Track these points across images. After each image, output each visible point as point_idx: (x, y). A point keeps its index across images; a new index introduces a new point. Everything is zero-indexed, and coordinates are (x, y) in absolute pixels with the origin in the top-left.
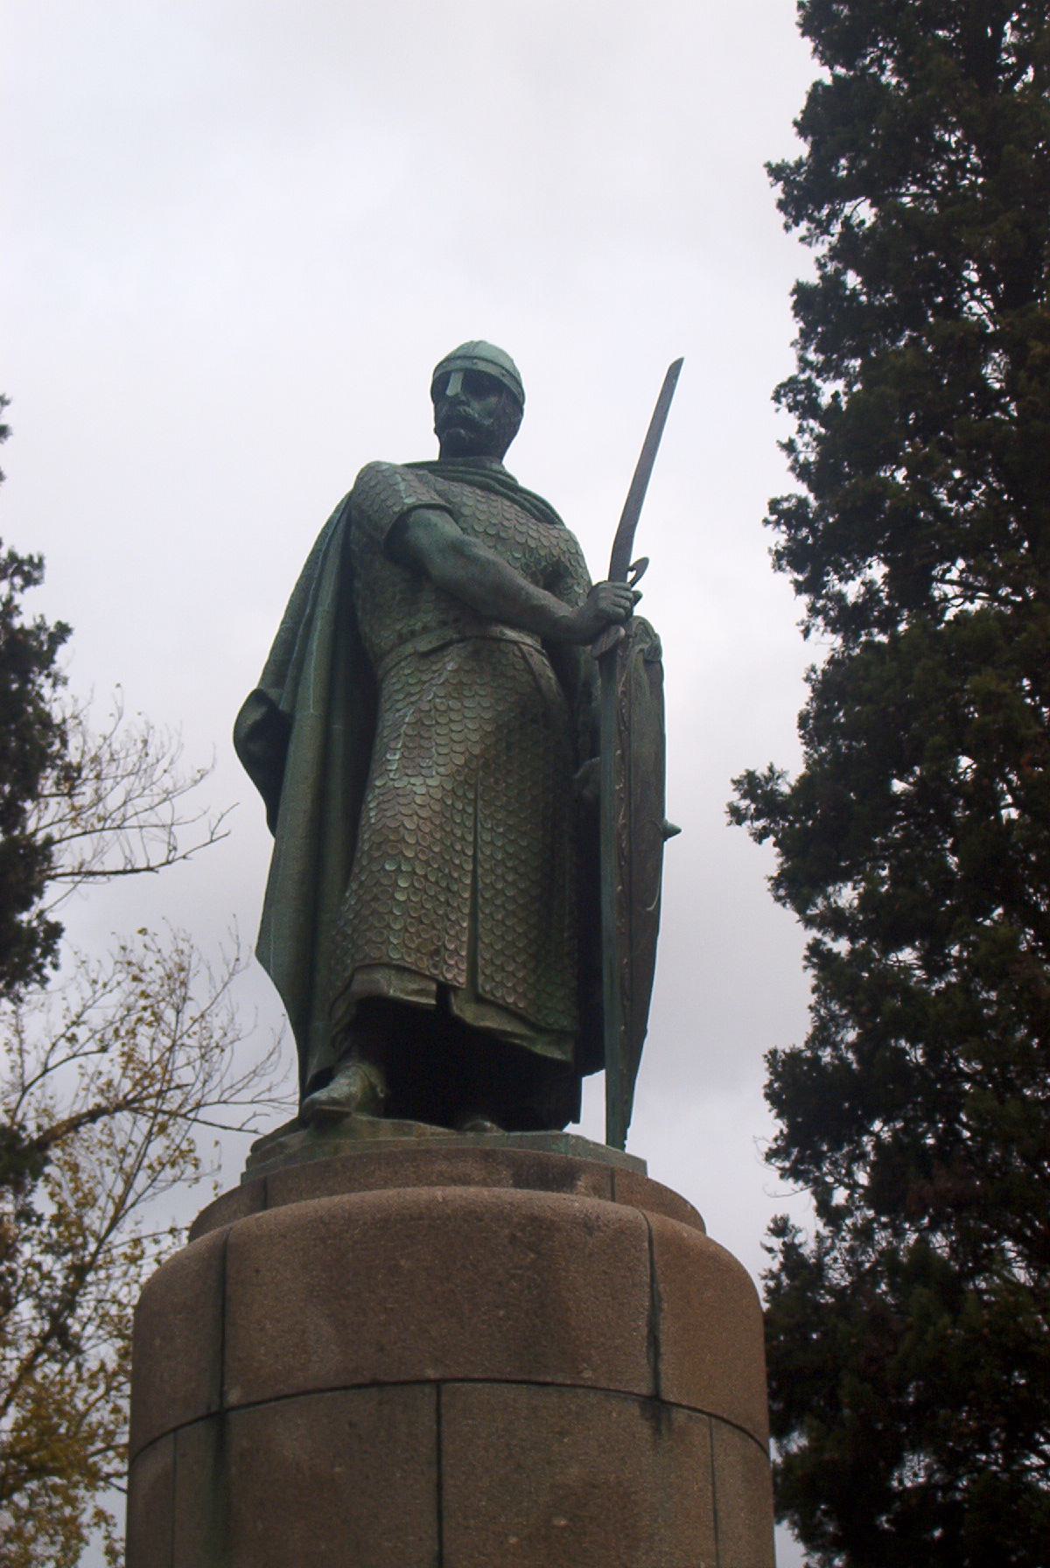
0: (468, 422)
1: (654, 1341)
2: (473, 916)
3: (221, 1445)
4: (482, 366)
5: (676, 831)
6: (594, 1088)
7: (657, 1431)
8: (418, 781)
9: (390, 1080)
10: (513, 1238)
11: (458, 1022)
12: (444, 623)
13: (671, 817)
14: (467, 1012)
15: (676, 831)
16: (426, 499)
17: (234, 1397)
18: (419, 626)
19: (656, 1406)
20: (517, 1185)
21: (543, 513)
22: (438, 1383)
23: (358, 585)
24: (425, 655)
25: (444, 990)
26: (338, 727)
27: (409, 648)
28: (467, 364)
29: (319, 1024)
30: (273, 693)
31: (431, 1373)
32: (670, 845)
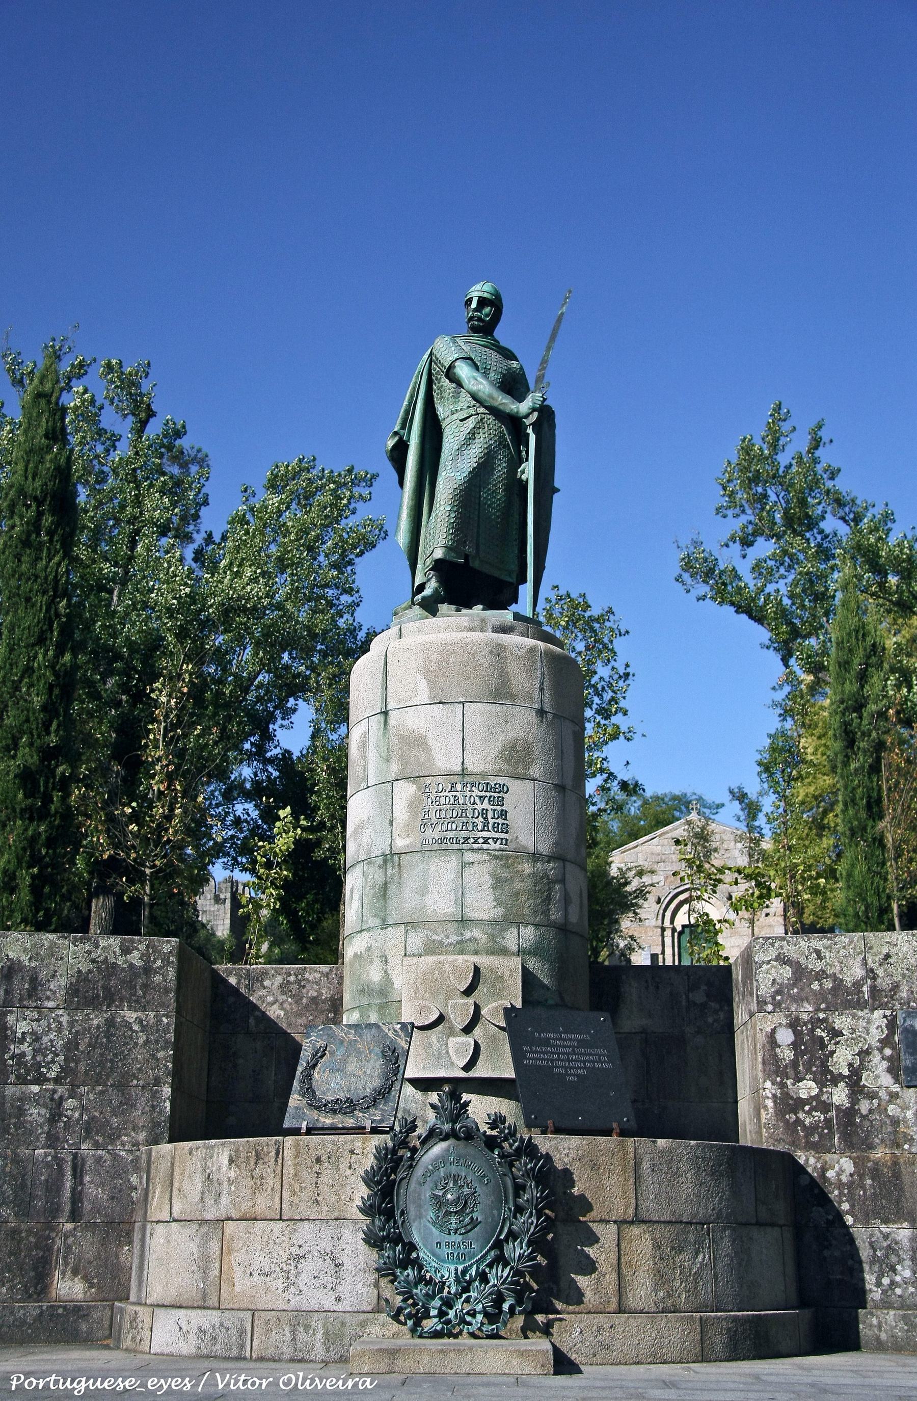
0: (480, 319)
1: (541, 689)
2: (479, 526)
3: (386, 721)
4: (486, 295)
5: (558, 490)
6: (526, 590)
7: (542, 721)
8: (458, 474)
9: (445, 590)
10: (491, 652)
11: (472, 568)
12: (469, 407)
13: (557, 485)
14: (476, 564)
15: (558, 490)
16: (463, 355)
17: (389, 707)
18: (459, 408)
19: (541, 712)
20: (493, 632)
21: (508, 355)
22: (463, 703)
23: (435, 387)
24: (461, 420)
25: (466, 557)
26: (427, 446)
27: (455, 417)
28: (480, 294)
29: (419, 566)
30: (402, 432)
31: (461, 700)
32: (556, 497)
